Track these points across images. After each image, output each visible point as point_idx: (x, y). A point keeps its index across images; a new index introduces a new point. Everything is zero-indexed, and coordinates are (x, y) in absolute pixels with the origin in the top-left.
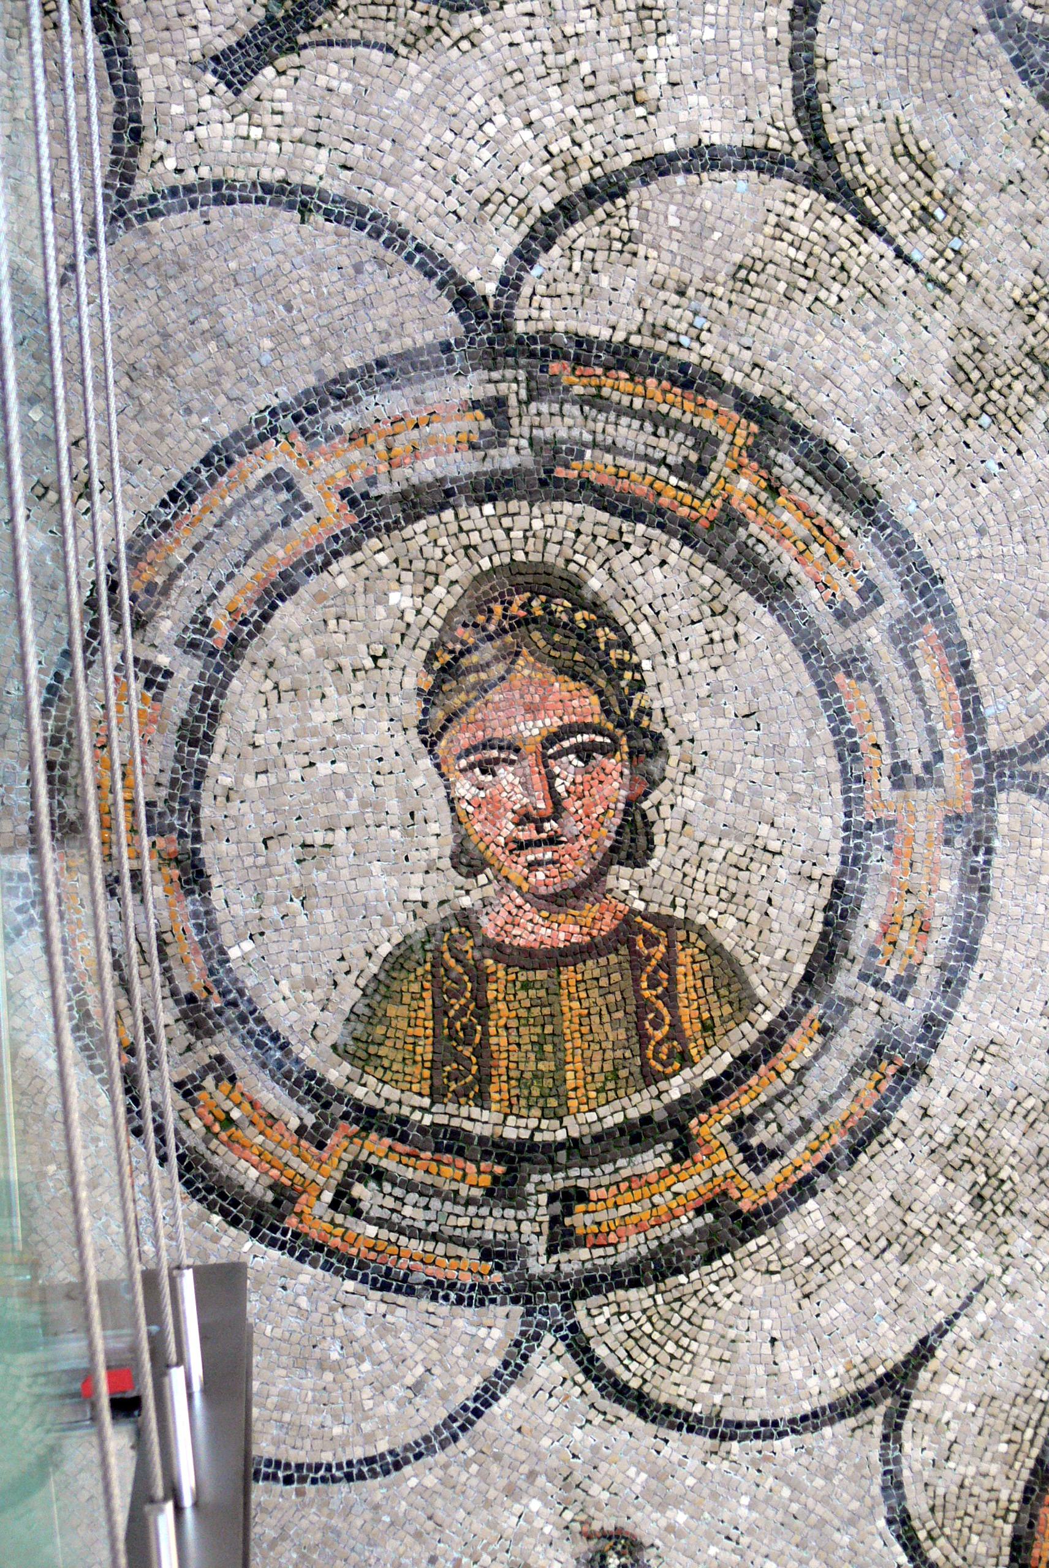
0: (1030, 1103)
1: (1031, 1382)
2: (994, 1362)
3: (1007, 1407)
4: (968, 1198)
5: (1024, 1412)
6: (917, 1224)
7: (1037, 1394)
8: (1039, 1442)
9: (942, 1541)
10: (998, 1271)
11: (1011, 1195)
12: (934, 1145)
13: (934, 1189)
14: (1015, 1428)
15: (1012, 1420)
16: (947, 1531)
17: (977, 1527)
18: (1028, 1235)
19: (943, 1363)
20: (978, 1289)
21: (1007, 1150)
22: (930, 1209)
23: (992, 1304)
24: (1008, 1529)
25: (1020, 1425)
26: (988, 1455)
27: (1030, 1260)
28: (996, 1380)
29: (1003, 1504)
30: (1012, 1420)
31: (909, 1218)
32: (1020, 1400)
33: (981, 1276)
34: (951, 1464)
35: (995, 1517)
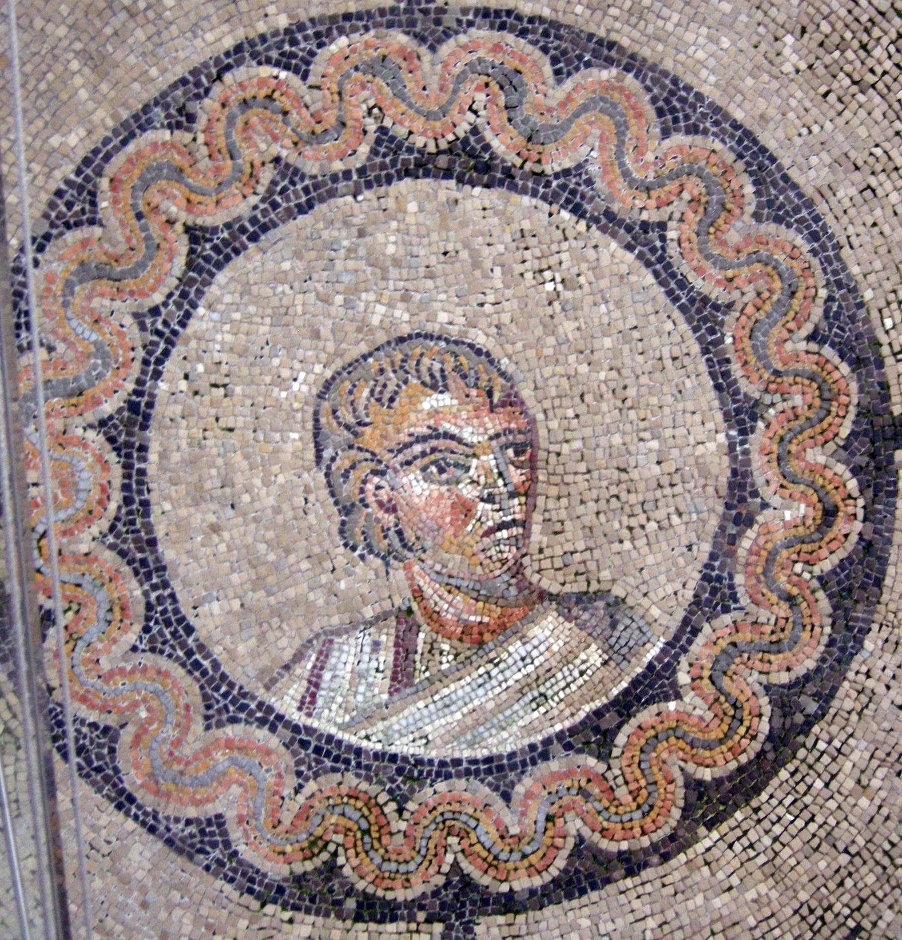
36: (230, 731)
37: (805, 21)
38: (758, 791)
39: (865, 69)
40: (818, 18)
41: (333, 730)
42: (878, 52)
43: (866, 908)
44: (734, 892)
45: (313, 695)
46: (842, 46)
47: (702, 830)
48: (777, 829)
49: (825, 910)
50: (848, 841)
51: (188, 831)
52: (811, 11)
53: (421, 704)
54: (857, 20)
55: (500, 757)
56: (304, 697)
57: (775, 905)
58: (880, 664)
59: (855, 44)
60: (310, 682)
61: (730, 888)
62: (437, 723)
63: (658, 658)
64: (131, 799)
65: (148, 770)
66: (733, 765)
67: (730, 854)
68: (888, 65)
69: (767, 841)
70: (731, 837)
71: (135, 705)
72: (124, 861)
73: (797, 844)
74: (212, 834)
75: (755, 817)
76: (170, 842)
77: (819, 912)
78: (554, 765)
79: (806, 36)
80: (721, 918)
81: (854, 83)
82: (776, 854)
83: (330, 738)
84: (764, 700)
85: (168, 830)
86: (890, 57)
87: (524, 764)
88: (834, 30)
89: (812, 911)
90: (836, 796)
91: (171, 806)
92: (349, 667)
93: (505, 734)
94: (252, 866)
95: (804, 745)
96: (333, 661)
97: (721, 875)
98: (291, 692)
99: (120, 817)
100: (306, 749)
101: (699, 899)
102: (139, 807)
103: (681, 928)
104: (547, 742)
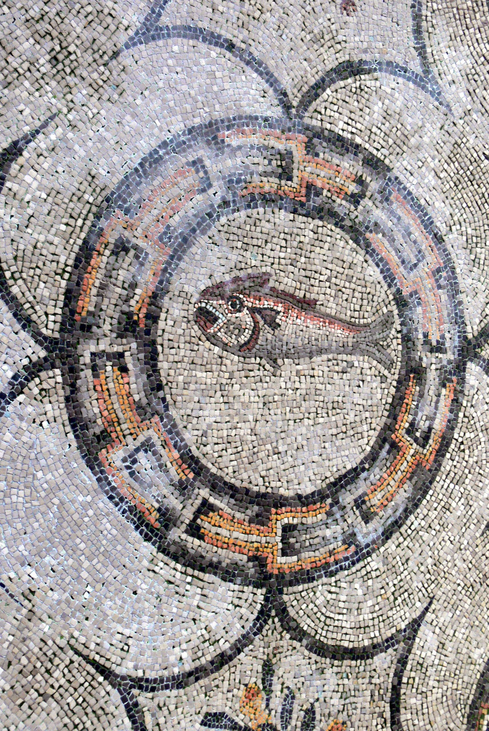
0: (89, 9)
1: (82, 188)
2: (60, 169)
3: (67, 201)
4: (48, 57)
5: (78, 207)
6: (15, 65)
7: (86, 197)
8: (86, 229)
9: (20, 282)
10: (65, 110)
11: (75, 63)
12: (28, 17)
13: (26, 45)
14: (71, 217)
15: (69, 210)
16: (24, 275)
17: (44, 278)
18: (84, 92)
19: (27, 161)
20: (52, 118)
21: (74, 34)
22: (24, 58)
23: (60, 130)
24: (64, 283)
25: (75, 215)
26: (53, 230)
27: (84, 108)
28: (60, 181)
29: (61, 266)
30: (69, 210)
31: (10, 59)
32: (75, 198)
33: (54, 111)
34: (29, 230)
35: (57, 274)
37: (11, 657)
39: (48, 685)
40: (20, 655)
42: (57, 674)
46: (34, 672)
52: (16, 650)
54: (45, 654)
59: (43, 670)
68: (63, 681)
79: (11, 667)
81: (40, 695)
86: (64, 676)
88: (30, 661)
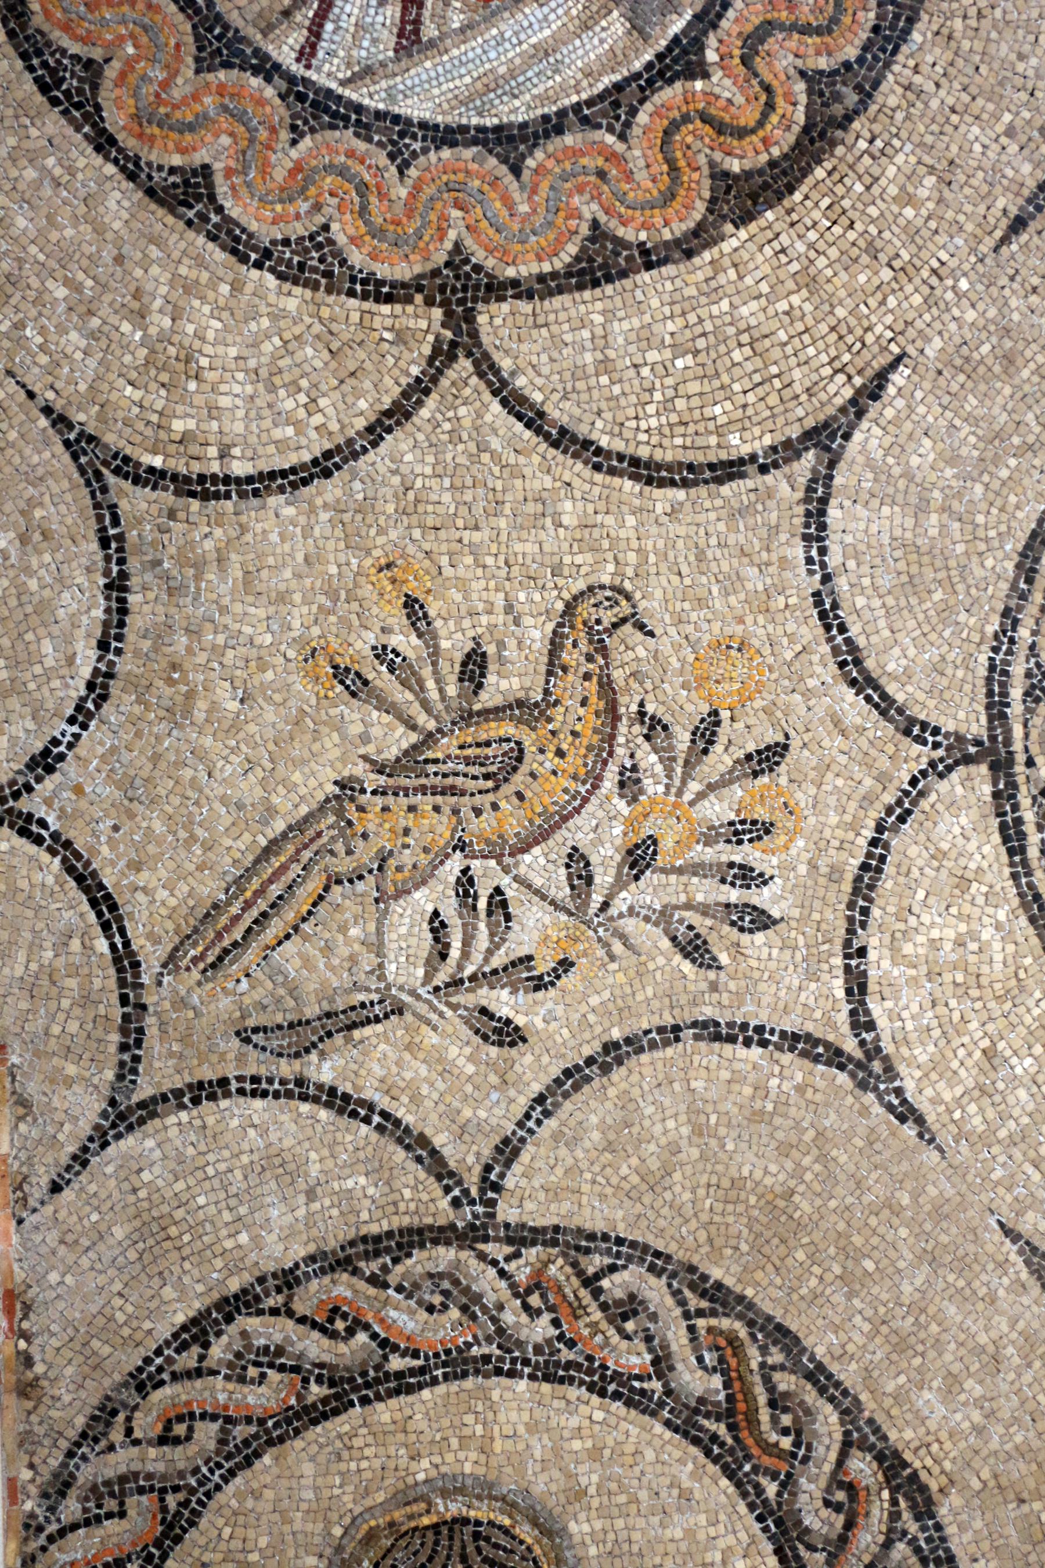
36: (222, 75)
38: (791, 189)
41: (333, 85)
43: (911, 333)
44: (763, 300)
45: (313, 47)
47: (729, 228)
48: (812, 236)
49: (867, 330)
50: (891, 253)
51: (171, 179)
53: (428, 64)
55: (511, 125)
56: (303, 47)
57: (809, 321)
58: (930, 59)
60: (310, 30)
61: (761, 295)
62: (444, 87)
63: (684, 32)
64: (112, 141)
65: (133, 110)
66: (764, 158)
67: (760, 258)
69: (800, 247)
70: (761, 239)
71: (121, 39)
72: (101, 209)
73: (833, 253)
74: (197, 185)
75: (788, 219)
76: (150, 192)
77: (859, 332)
78: (568, 139)
80: (748, 329)
82: (811, 262)
83: (329, 92)
84: (800, 86)
85: (150, 177)
87: (536, 137)
89: (850, 331)
90: (879, 202)
91: (155, 152)
92: (353, 20)
93: (517, 103)
94: (238, 225)
95: (843, 142)
96: (336, 10)
97: (749, 281)
98: (291, 41)
99: (99, 160)
100: (303, 102)
101: (725, 305)
102: (120, 150)
103: (704, 334)
104: (562, 113)
